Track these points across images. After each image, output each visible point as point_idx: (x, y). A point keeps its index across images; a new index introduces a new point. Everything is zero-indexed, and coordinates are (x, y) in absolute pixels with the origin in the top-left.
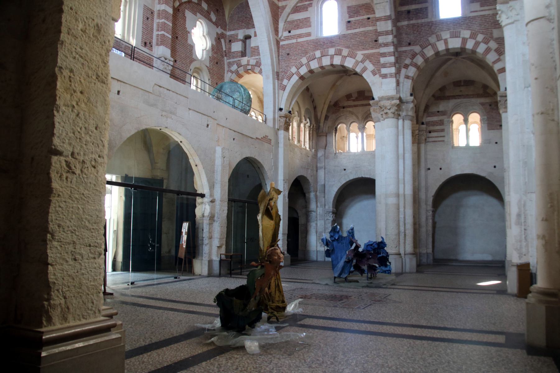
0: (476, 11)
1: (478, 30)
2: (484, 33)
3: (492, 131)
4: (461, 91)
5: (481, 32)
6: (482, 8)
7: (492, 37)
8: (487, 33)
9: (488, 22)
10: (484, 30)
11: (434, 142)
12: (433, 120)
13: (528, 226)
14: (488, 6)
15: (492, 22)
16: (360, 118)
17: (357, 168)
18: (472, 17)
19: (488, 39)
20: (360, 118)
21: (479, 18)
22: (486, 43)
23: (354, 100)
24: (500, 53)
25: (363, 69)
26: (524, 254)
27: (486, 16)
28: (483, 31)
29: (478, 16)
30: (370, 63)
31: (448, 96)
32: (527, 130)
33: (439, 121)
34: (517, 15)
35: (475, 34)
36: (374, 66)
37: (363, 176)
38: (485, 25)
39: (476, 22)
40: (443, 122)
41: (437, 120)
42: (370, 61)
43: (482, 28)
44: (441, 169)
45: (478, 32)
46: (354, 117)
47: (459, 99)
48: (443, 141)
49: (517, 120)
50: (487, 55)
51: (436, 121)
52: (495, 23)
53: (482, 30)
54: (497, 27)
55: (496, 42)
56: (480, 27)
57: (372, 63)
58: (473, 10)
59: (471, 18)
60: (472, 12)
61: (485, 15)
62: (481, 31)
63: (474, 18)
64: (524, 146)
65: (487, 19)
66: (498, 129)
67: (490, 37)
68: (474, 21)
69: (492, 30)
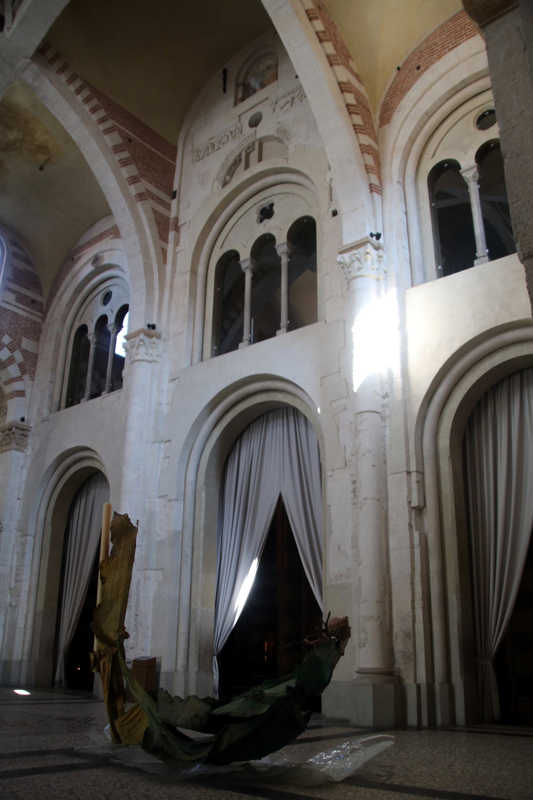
0: (10, 304)
1: (6, 328)
2: (12, 336)
5: (9, 333)
6: (17, 304)
7: (20, 346)
8: (15, 337)
9: (19, 324)
10: (12, 332)
13: (140, 611)
14: (23, 304)
15: (23, 327)
18: (4, 308)
19: (15, 346)
21: (11, 315)
22: (12, 350)
24: (24, 371)
26: (130, 647)
27: (19, 316)
28: (11, 333)
29: (10, 311)
32: (154, 493)
34: (158, 356)
35: (2, 332)
38: (16, 326)
39: (7, 318)
43: (12, 328)
45: (6, 331)
49: (140, 477)
50: (8, 366)
52: (27, 330)
53: (11, 330)
54: (28, 336)
55: (22, 354)
56: (9, 326)
58: (6, 300)
59: (2, 308)
60: (4, 301)
61: (18, 314)
62: (9, 331)
63: (5, 310)
64: (145, 510)
65: (20, 321)
67: (17, 345)
68: (4, 314)
69: (21, 337)
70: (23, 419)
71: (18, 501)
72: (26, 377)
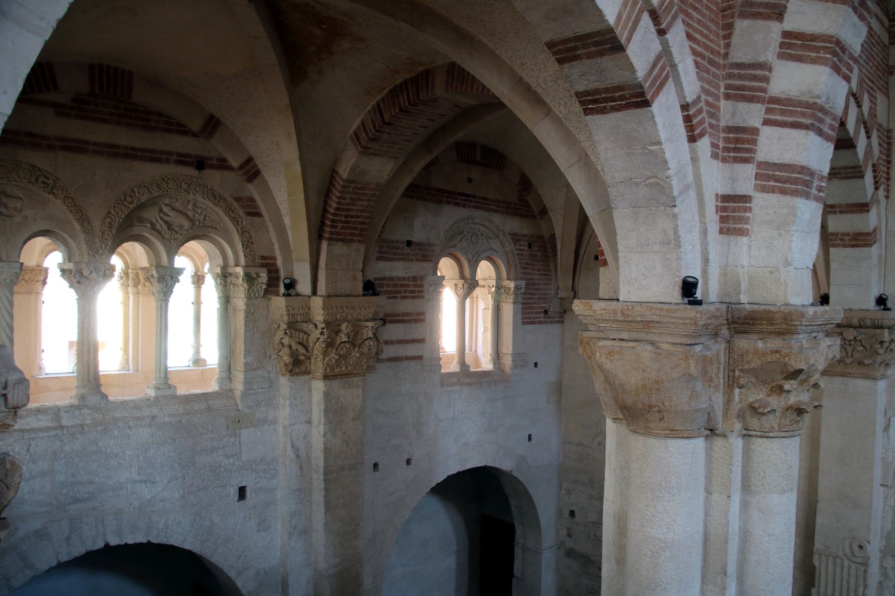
3: (531, 327)
4: (470, 180)
11: (394, 364)
12: (394, 274)
16: (97, 224)
17: (76, 501)
20: (97, 224)
23: (62, 111)
25: (654, 66)
30: (687, 43)
31: (438, 190)
33: (408, 279)
36: (700, 78)
37: (114, 541)
40: (422, 286)
41: (406, 275)
42: (689, 36)
44: (408, 462)
46: (57, 206)
47: (464, 206)
48: (420, 358)
51: (404, 279)
57: (694, 52)
66: (540, 323)
70: (881, 301)
71: (882, 488)
72: (881, 192)
